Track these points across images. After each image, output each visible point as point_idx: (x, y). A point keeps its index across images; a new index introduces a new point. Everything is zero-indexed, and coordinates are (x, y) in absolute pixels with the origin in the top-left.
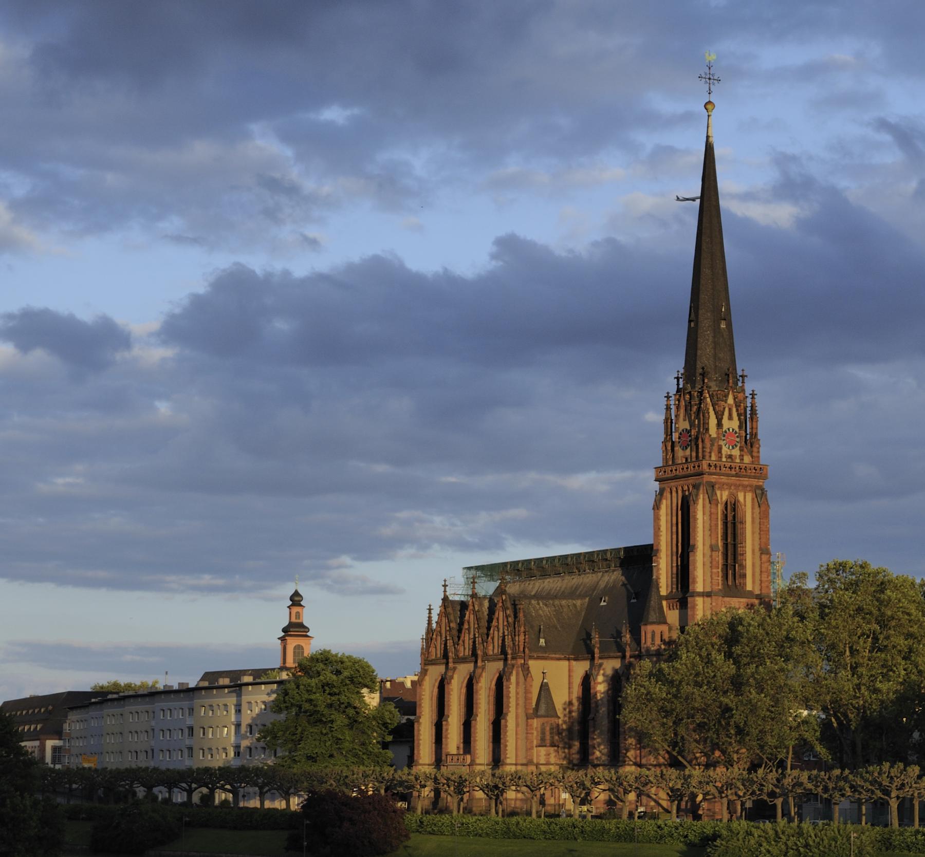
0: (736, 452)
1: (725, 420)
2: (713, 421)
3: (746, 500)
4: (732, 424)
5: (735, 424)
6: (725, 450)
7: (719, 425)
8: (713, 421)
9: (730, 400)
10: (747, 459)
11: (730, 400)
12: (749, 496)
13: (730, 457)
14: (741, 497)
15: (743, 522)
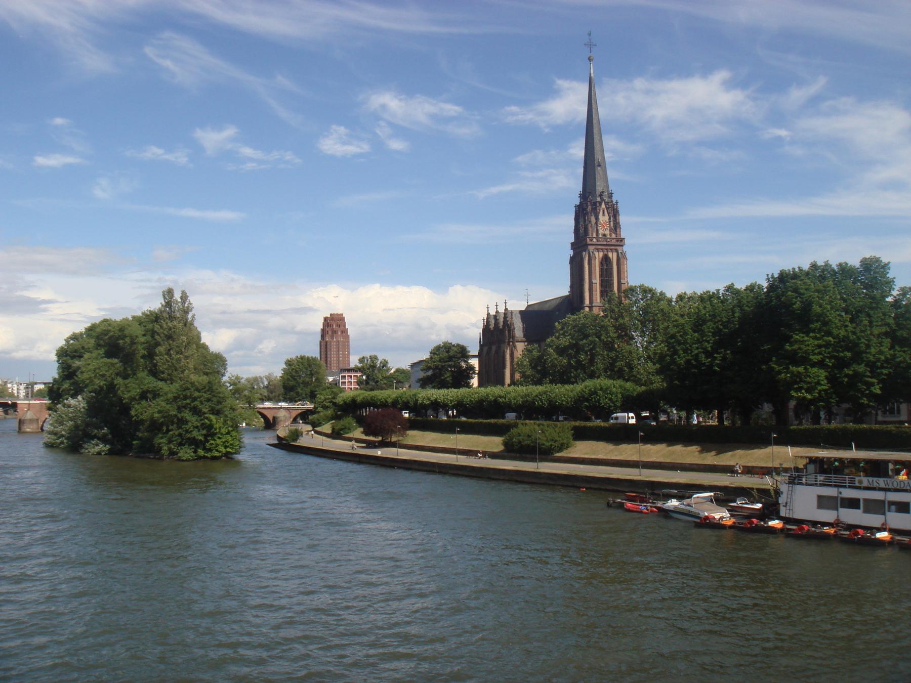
0: (607, 232)
1: (601, 216)
2: (593, 219)
3: (613, 256)
4: (604, 218)
5: (606, 218)
6: (601, 232)
7: (597, 219)
8: (593, 219)
9: (603, 206)
10: (614, 236)
11: (603, 206)
12: (615, 254)
13: (604, 235)
14: (610, 254)
15: (612, 269)
